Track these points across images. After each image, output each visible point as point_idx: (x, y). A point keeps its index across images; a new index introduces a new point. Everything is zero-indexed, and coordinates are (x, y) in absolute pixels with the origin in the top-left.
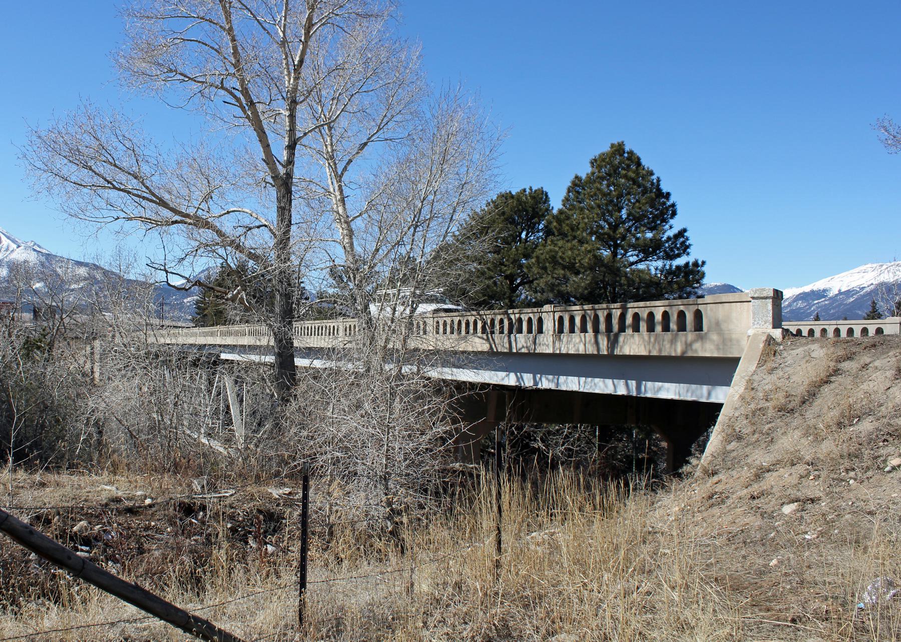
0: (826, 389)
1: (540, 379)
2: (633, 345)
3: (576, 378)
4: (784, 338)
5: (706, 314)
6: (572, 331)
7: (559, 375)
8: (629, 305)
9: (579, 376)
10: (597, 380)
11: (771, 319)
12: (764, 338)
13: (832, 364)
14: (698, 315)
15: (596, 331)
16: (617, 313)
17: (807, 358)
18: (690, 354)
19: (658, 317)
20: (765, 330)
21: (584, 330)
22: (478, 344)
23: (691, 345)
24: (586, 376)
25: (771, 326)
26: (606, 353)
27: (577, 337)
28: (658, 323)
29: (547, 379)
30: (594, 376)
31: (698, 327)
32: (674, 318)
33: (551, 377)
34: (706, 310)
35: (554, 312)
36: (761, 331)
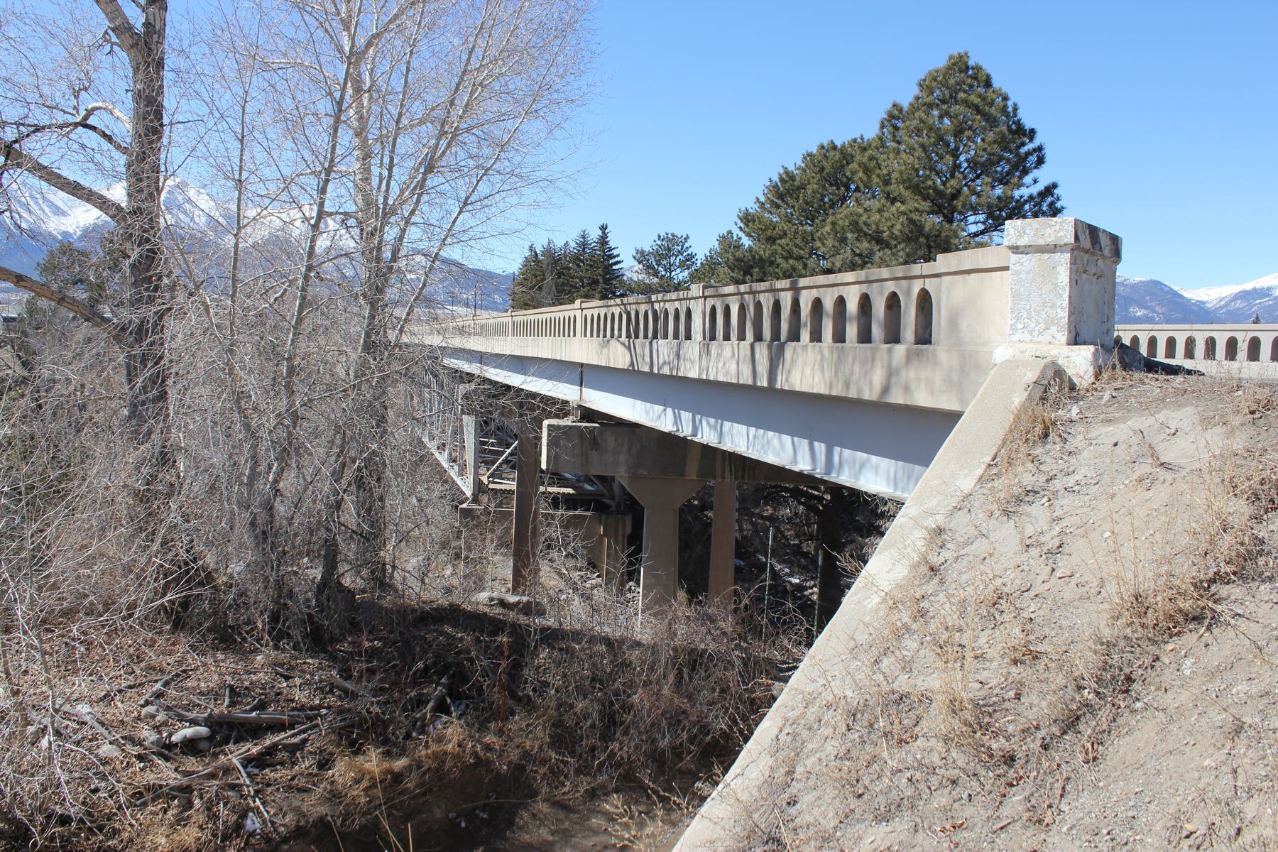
0: (1192, 656)
1: (701, 421)
2: (807, 370)
3: (744, 427)
4: (1097, 375)
5: (939, 300)
6: (727, 337)
7: (723, 420)
8: (803, 282)
9: (748, 424)
10: (770, 434)
11: (1063, 314)
12: (1031, 375)
13: (1240, 509)
14: (925, 301)
15: (758, 337)
16: (786, 299)
17: (1145, 468)
18: (897, 398)
19: (852, 306)
20: (1043, 350)
21: (666, 337)
22: (617, 356)
23: (898, 372)
24: (757, 427)
25: (1063, 337)
26: (765, 384)
27: (728, 348)
28: (828, 315)
29: (708, 423)
30: (767, 428)
31: (924, 337)
32: (879, 308)
33: (712, 421)
34: (939, 289)
35: (705, 298)
36: (1031, 350)
